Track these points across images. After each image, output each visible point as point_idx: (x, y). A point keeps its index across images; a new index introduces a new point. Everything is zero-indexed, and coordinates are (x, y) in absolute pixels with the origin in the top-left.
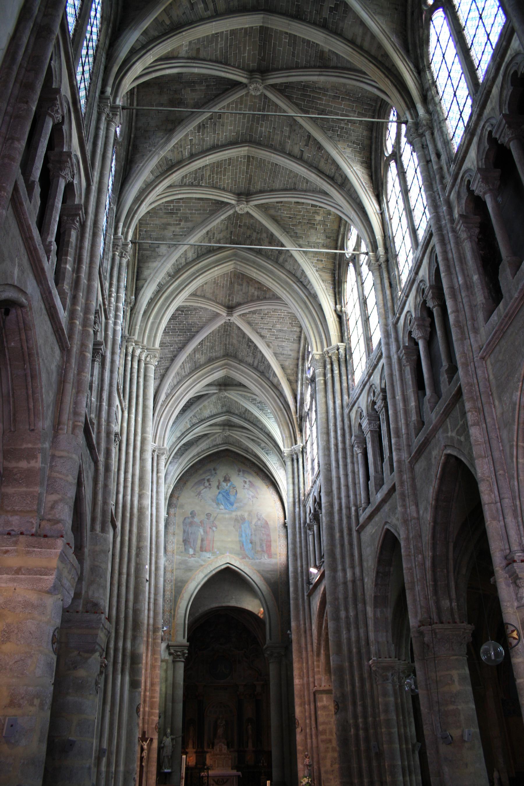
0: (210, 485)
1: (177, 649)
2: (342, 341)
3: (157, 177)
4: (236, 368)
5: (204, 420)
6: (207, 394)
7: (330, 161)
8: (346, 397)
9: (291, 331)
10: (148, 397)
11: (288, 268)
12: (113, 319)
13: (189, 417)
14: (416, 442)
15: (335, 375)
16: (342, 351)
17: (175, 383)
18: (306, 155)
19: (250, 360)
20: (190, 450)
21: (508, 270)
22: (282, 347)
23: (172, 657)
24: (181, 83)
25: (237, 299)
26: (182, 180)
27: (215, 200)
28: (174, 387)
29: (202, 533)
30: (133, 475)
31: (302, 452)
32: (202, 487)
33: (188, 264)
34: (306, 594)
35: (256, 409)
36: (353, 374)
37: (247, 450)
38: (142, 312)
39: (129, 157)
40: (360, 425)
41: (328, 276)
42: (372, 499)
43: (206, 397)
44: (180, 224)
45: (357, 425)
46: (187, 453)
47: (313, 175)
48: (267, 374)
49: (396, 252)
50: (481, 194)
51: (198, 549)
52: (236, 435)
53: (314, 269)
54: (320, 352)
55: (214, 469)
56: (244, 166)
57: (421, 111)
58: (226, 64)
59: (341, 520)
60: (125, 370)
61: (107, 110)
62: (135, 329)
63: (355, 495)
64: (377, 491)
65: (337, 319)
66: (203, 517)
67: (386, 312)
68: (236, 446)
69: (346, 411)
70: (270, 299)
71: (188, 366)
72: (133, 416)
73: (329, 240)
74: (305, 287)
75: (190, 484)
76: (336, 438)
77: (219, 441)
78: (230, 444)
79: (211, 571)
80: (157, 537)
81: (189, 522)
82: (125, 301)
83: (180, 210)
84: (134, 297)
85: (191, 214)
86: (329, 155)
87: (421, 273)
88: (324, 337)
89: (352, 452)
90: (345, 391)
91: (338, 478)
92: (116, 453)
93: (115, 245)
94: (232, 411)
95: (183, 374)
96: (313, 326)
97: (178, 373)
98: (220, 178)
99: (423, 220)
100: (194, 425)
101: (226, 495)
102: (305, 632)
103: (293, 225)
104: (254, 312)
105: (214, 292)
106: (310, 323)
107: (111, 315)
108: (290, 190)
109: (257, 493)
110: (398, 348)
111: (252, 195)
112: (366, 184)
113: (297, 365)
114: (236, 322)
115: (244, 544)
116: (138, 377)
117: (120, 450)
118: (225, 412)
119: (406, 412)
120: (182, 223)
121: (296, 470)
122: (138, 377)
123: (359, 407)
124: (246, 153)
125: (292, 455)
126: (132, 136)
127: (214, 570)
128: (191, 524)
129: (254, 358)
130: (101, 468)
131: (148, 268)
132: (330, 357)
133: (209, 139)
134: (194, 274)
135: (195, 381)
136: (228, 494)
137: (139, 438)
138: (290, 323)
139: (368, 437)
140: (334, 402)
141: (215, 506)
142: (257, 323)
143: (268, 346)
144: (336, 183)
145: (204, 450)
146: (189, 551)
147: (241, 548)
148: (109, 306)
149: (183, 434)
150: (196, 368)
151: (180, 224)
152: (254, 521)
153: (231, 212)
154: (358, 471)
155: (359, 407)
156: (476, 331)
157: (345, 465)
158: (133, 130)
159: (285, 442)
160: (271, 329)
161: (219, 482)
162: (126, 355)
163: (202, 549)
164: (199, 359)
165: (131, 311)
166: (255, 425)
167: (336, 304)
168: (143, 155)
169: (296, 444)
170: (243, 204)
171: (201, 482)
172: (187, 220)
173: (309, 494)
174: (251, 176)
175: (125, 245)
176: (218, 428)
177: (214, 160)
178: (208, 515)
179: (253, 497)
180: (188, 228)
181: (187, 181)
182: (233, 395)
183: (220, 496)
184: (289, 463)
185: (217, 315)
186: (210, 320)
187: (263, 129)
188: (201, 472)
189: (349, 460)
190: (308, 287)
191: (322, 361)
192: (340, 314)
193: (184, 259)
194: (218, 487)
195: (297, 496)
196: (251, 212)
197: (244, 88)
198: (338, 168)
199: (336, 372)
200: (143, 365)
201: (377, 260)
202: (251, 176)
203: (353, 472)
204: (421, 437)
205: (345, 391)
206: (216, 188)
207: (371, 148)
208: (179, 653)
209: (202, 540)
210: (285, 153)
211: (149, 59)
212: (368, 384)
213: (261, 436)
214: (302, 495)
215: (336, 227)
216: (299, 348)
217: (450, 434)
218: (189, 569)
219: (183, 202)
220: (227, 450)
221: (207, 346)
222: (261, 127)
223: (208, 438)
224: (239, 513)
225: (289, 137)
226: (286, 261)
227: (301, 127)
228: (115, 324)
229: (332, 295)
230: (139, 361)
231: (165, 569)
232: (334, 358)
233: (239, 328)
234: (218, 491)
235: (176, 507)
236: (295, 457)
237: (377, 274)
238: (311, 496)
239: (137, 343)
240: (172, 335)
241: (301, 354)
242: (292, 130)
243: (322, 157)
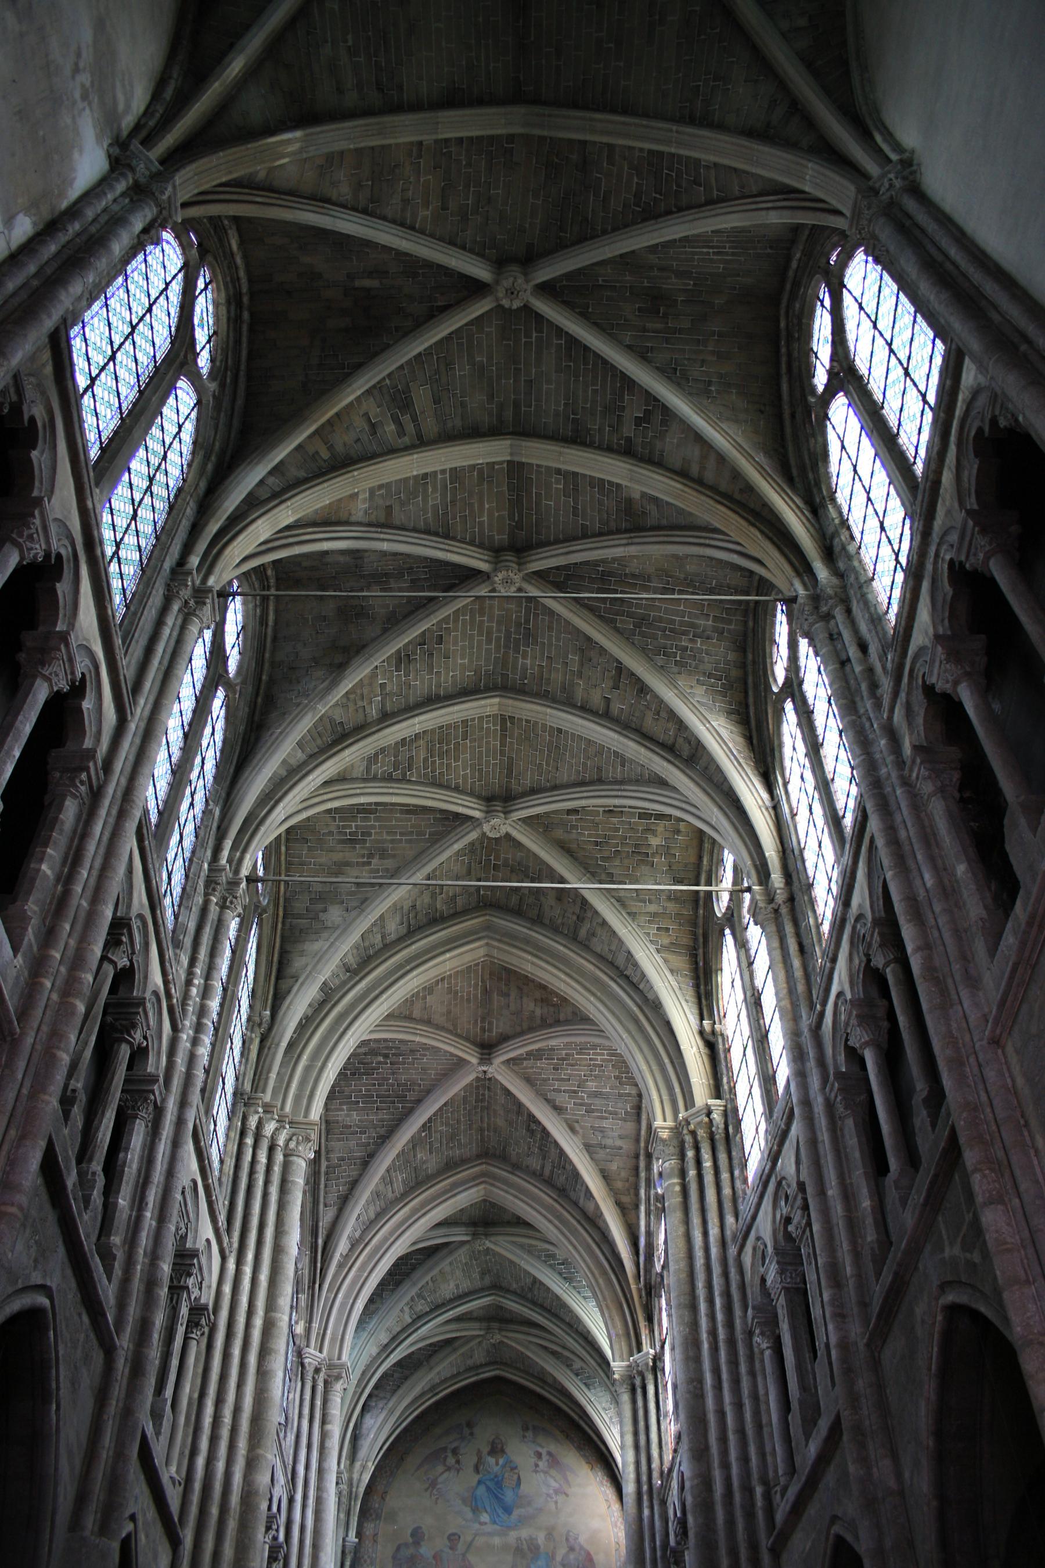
0: (458, 1462)
2: (718, 1095)
3: (312, 756)
4: (505, 1182)
5: (443, 1305)
6: (447, 1244)
7: (663, 714)
8: (730, 1219)
9: (620, 1095)
10: (286, 1228)
11: (598, 950)
12: (191, 1032)
13: (408, 1298)
14: (878, 1291)
15: (704, 1172)
16: (717, 1116)
17: (372, 1216)
18: (616, 707)
19: (535, 1163)
21: (1023, 821)
22: (602, 1130)
24: (363, 577)
25: (499, 1026)
26: (368, 769)
27: (442, 811)
28: (370, 1226)
30: (237, 1410)
31: (654, 1369)
32: (440, 1468)
33: (388, 947)
35: (557, 1278)
36: (744, 1166)
37: (543, 1378)
38: (284, 1044)
39: (256, 718)
40: (763, 1280)
41: (681, 962)
42: (798, 1459)
43: (445, 1251)
44: (369, 863)
45: (757, 1281)
46: (408, 1384)
47: (631, 744)
48: (572, 1195)
49: (808, 878)
50: (948, 687)
52: (517, 1341)
53: (652, 948)
54: (670, 1123)
55: (469, 1425)
56: (495, 740)
57: (822, 573)
58: (447, 536)
59: (730, 1522)
60: (237, 1167)
61: (186, 593)
62: (267, 1078)
63: (762, 1454)
64: (808, 1436)
65: (704, 1050)
67: (795, 1005)
69: (732, 1251)
70: (567, 1022)
71: (399, 1178)
72: (248, 1270)
74: (635, 987)
76: (712, 1316)
77: (479, 1357)
78: (505, 1364)
82: (249, 1020)
83: (370, 834)
84: (268, 1013)
85: (392, 841)
86: (661, 701)
87: (855, 901)
88: (677, 1090)
89: (750, 1346)
90: (728, 1205)
91: (721, 1413)
92: (198, 1353)
93: (211, 883)
95: (390, 1195)
96: (655, 1068)
97: (377, 1194)
98: (449, 766)
99: (846, 792)
100: (419, 1317)
101: (496, 1488)
103: (603, 859)
104: (537, 1055)
105: (449, 1012)
106: (648, 1062)
107: (187, 1023)
108: (591, 783)
110: (825, 1080)
111: (515, 799)
112: (739, 752)
113: (637, 1169)
114: (499, 1078)
116: (267, 1183)
117: (210, 1347)
118: (489, 1288)
119: (853, 1224)
120: (374, 861)
121: (641, 1413)
122: (267, 1183)
123: (758, 1238)
124: (495, 710)
125: (632, 1378)
126: (264, 677)
129: (544, 1158)
130: (122, 1365)
131: (302, 953)
132: (693, 1133)
133: (421, 683)
134: (400, 966)
135: (414, 1211)
136: (499, 1484)
137: (258, 1322)
139: (781, 1303)
140: (705, 1234)
141: (469, 1515)
142: (545, 1080)
143: (572, 1129)
144: (678, 756)
145: (446, 1380)
148: (184, 1004)
149: (393, 1339)
150: (418, 1182)
151: (369, 863)
152: (561, 1553)
153: (474, 835)
154: (767, 1394)
155: (758, 1238)
156: (973, 982)
157: (736, 1381)
158: (267, 666)
159: (616, 1347)
160: (575, 1092)
161: (479, 1453)
162: (243, 1134)
164: (424, 1162)
165: (262, 1041)
166: (556, 1316)
167: (702, 1019)
168: (284, 714)
169: (639, 1350)
170: (498, 817)
171: (436, 1456)
172: (383, 854)
173: (670, 1470)
174: (510, 758)
175: (234, 884)
176: (477, 1325)
177: (429, 726)
178: (453, 1539)
180: (387, 870)
181: (378, 769)
182: (502, 1246)
183: (481, 1490)
184: (625, 1398)
185: (461, 1063)
186: (445, 1075)
187: (529, 662)
189: (743, 1369)
190: (641, 987)
191: (675, 1143)
192: (711, 1038)
193: (379, 936)
194: (477, 1469)
195: (644, 1478)
196: (514, 834)
197: (484, 582)
198: (681, 725)
199: (707, 1164)
200: (279, 1157)
201: (771, 900)
202: (510, 758)
203: (755, 1397)
204: (887, 1277)
205: (728, 1205)
206: (441, 786)
207: (746, 683)
210: (574, 706)
211: (286, 514)
212: (773, 1180)
213: (570, 1342)
214: (656, 1474)
215: (693, 859)
216: (639, 1130)
217: (947, 1253)
219: (377, 819)
221: (441, 1132)
222: (524, 657)
223: (455, 1350)
224: (524, 1533)
225: (580, 675)
226: (594, 935)
227: (603, 651)
228: (195, 1042)
229: (692, 999)
230: (272, 1149)
232: (701, 1133)
233: (508, 1093)
234: (476, 1478)
235: (378, 1517)
236: (638, 1382)
237: (772, 928)
238: (675, 1474)
239: (268, 1109)
240: (363, 1109)
242: (585, 660)
243: (648, 707)
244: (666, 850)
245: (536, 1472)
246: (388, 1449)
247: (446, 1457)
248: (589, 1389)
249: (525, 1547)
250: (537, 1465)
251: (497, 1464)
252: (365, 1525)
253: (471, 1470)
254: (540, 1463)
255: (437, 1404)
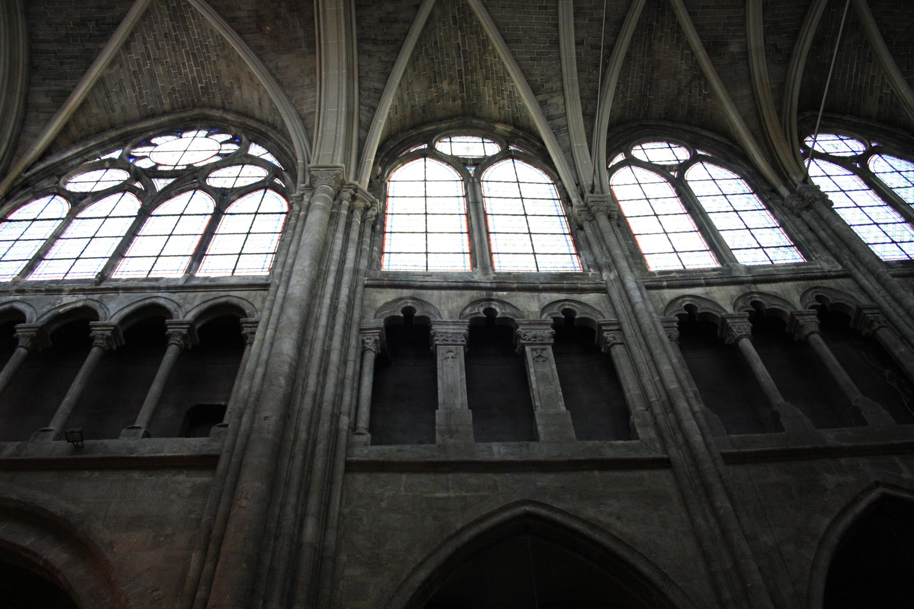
9: (159, 96)
22: (122, 89)
73: (421, 111)
138: (173, 89)
160: (149, 57)
241: (129, 129)
244: (441, 95)
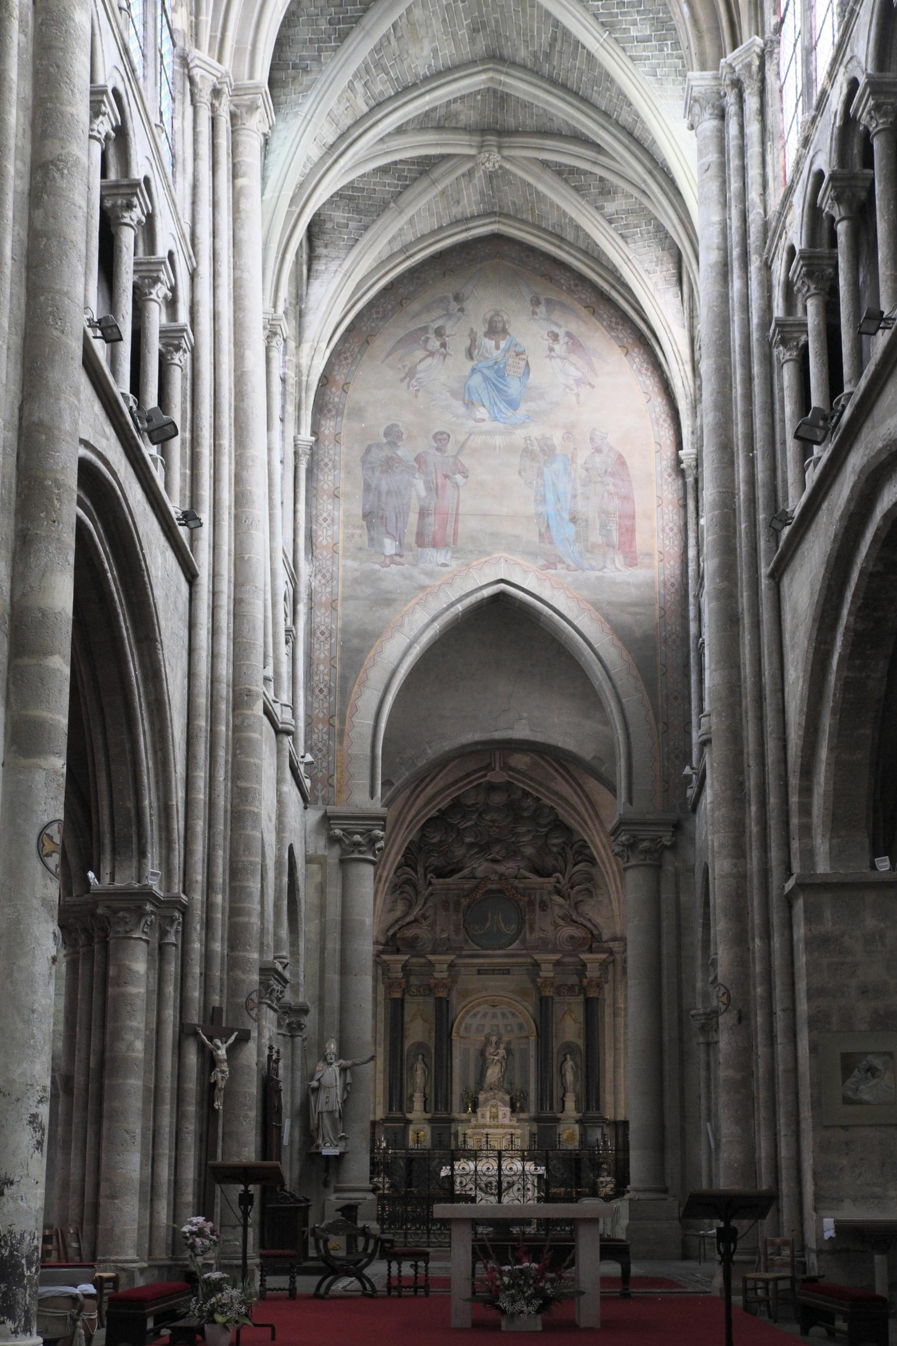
0: (443, 345)
1: (350, 825)
20: (375, 228)
23: (336, 851)
29: (423, 493)
32: (420, 354)
34: (764, 571)
46: (368, 235)
51: (411, 539)
66: (424, 444)
68: (524, 222)
75: (382, 344)
78: (507, 216)
79: (452, 605)
80: (240, 394)
81: (382, 457)
94: (507, 52)
102: (760, 700)
109: (593, 370)
115: (553, 523)
127: (459, 600)
128: (389, 464)
136: (501, 374)
141: (462, 410)
145: (423, 237)
146: (382, 545)
147: (541, 535)
152: (584, 453)
163: (421, 540)
166: (585, 100)
176: (465, 138)
178: (441, 438)
179: (579, 382)
183: (477, 380)
188: (415, 306)
194: (470, 354)
208: (357, 838)
209: (423, 514)
218: (386, 600)
220: (496, 238)
224: (535, 431)
231: (310, 597)
234: (470, 365)
235: (339, 413)
245: (550, 357)
246: (348, 330)
247: (427, 340)
248: (626, 242)
249: (536, 448)
250: (551, 350)
251: (497, 347)
252: (323, 422)
253: (462, 355)
254: (556, 347)
255: (412, 272)
